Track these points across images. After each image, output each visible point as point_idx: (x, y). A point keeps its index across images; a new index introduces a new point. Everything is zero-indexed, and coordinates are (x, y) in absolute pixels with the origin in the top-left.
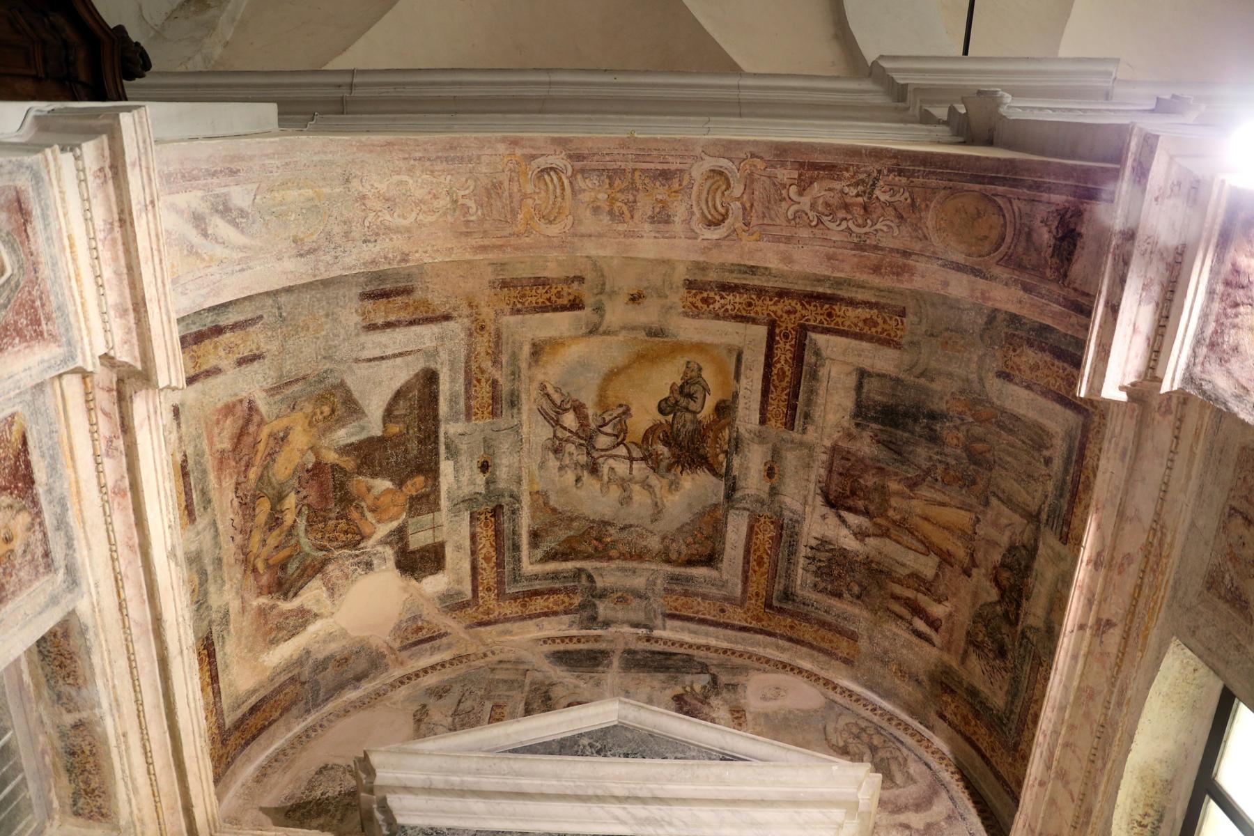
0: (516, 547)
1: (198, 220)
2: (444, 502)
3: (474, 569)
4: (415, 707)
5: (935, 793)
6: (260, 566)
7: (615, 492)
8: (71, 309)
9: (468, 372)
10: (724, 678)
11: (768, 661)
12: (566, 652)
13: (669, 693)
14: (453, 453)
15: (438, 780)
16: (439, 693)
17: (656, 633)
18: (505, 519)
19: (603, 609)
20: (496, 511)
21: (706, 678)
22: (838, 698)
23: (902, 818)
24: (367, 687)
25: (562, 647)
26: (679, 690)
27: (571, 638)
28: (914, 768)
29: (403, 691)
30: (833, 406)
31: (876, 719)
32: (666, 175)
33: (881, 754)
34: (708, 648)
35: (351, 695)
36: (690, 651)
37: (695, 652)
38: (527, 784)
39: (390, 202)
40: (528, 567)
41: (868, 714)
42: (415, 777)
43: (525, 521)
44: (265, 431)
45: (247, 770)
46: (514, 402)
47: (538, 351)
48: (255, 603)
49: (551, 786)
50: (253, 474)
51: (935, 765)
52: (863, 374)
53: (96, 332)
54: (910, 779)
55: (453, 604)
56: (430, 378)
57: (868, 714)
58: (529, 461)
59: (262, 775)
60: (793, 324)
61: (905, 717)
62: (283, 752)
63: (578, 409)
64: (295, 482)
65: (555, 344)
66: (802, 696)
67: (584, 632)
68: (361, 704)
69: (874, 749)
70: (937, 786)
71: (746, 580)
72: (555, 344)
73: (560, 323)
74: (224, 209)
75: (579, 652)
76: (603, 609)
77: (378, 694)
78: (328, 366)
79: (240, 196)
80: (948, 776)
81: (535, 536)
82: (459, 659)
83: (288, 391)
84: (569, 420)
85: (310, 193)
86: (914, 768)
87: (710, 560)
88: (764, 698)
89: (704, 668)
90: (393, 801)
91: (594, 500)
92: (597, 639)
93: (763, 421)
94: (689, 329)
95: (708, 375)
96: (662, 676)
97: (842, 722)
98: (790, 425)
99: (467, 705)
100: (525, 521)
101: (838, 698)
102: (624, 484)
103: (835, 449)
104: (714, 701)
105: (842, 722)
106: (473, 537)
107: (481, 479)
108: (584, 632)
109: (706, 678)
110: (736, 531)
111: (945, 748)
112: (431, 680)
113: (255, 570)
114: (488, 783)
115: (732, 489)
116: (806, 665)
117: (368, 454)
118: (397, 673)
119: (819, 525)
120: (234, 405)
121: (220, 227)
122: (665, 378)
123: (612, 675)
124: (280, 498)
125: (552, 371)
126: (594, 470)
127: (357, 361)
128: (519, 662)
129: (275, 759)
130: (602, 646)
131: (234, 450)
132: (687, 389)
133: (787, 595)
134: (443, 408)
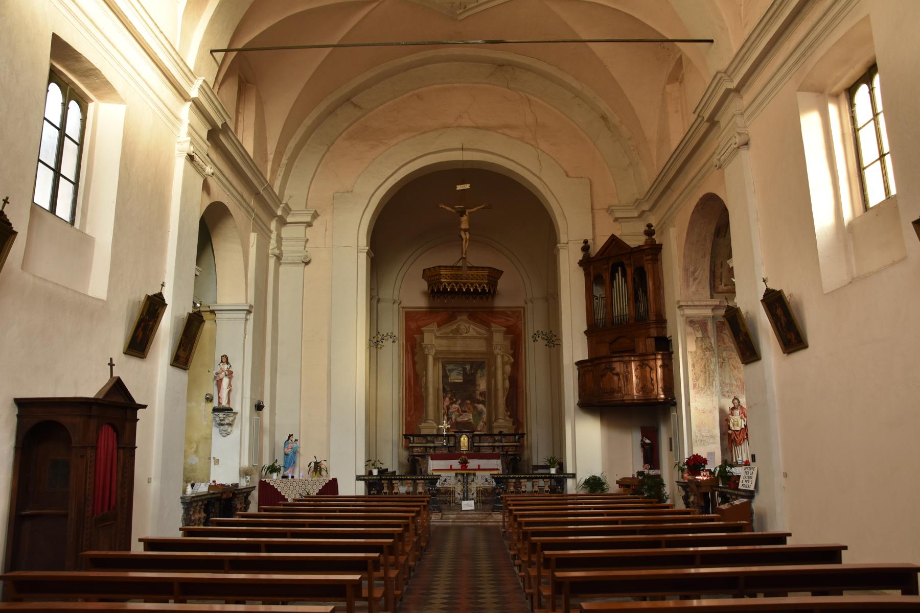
1: (695, 280)
53: (708, 312)
74: (694, 272)
79: (692, 269)
121: (697, 274)
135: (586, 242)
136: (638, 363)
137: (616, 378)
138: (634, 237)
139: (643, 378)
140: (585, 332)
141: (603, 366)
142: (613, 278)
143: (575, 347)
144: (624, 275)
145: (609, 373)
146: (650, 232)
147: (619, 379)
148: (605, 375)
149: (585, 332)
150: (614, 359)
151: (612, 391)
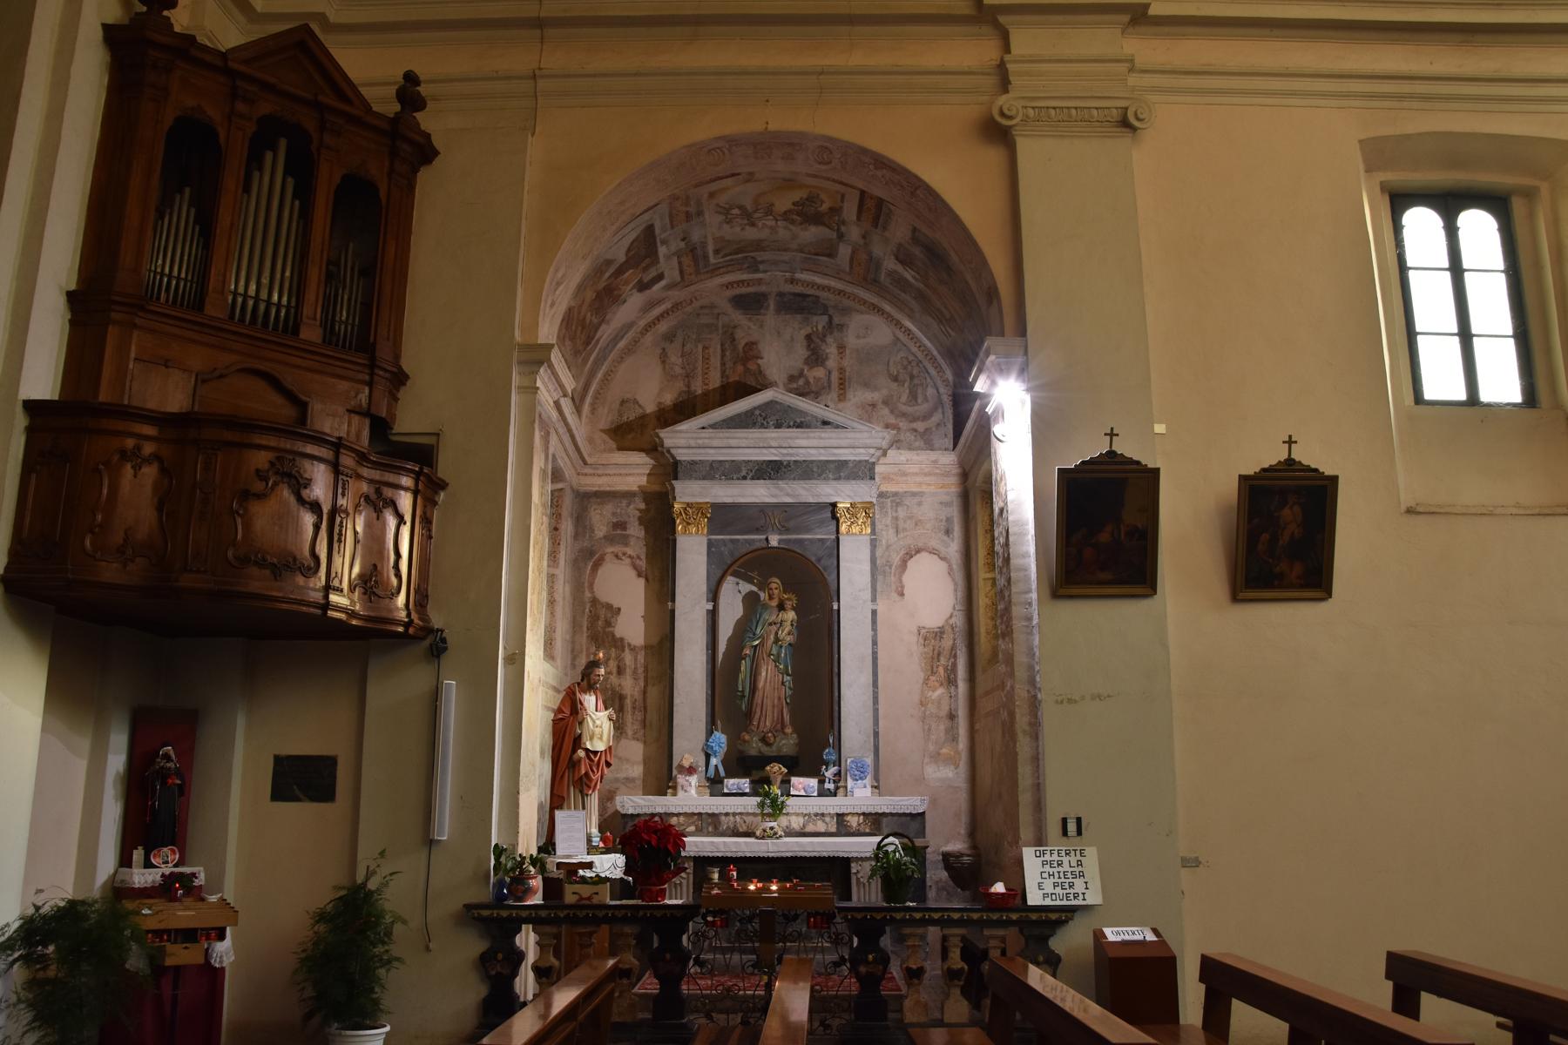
0: (706, 257)
2: (662, 259)
3: (681, 272)
4: (659, 351)
5: (935, 409)
7: (767, 231)
9: (671, 216)
10: (836, 320)
11: (865, 302)
12: (741, 296)
13: (804, 332)
14: (664, 242)
15: (692, 443)
16: (669, 337)
17: (798, 276)
18: (699, 252)
19: (761, 267)
20: (693, 250)
21: (826, 318)
22: (901, 336)
23: (914, 425)
24: (630, 335)
25: (738, 291)
26: (809, 330)
27: (743, 282)
28: (930, 391)
29: (649, 338)
30: (899, 231)
31: (919, 354)
32: (790, 144)
33: (916, 381)
34: (829, 289)
35: (622, 344)
36: (817, 293)
37: (823, 295)
38: (733, 442)
40: (712, 260)
41: (914, 350)
42: (682, 442)
43: (710, 248)
45: (586, 408)
46: (700, 213)
47: (712, 195)
49: (744, 443)
51: (942, 390)
52: (915, 230)
54: (926, 399)
55: (669, 287)
56: (650, 229)
57: (914, 350)
58: (711, 229)
59: (593, 410)
60: (875, 212)
61: (935, 353)
62: (597, 393)
63: (740, 207)
65: (723, 190)
66: (881, 334)
67: (751, 276)
68: (629, 351)
69: (912, 377)
70: (940, 403)
71: (851, 267)
72: (723, 190)
73: (729, 182)
74: (558, 284)
75: (748, 295)
76: (761, 267)
77: (636, 341)
79: (560, 275)
80: (947, 399)
81: (717, 252)
82: (676, 306)
84: (736, 211)
86: (930, 391)
87: (830, 255)
88: (858, 337)
89: (825, 310)
90: (673, 451)
91: (751, 234)
92: (760, 282)
93: (859, 219)
94: (810, 181)
95: (823, 196)
96: (799, 317)
97: (902, 354)
98: (875, 223)
99: (688, 347)
100: (710, 248)
101: (901, 336)
102: (771, 227)
103: (900, 245)
104: (829, 340)
105: (902, 354)
106: (680, 263)
107: (682, 245)
108: (751, 276)
109: (826, 318)
110: (844, 251)
111: (951, 378)
112: (663, 327)
114: (716, 443)
115: (841, 236)
116: (887, 308)
117: (620, 271)
118: (642, 323)
119: (890, 264)
122: (797, 195)
123: (770, 318)
125: (723, 199)
126: (753, 225)
128: (713, 306)
129: (595, 398)
130: (763, 289)
132: (812, 199)
133: (875, 281)
134: (657, 231)
136: (365, 487)
137: (308, 519)
139: (374, 544)
141: (261, 459)
145: (286, 493)
146: (410, 93)
148: (261, 496)
150: (310, 449)
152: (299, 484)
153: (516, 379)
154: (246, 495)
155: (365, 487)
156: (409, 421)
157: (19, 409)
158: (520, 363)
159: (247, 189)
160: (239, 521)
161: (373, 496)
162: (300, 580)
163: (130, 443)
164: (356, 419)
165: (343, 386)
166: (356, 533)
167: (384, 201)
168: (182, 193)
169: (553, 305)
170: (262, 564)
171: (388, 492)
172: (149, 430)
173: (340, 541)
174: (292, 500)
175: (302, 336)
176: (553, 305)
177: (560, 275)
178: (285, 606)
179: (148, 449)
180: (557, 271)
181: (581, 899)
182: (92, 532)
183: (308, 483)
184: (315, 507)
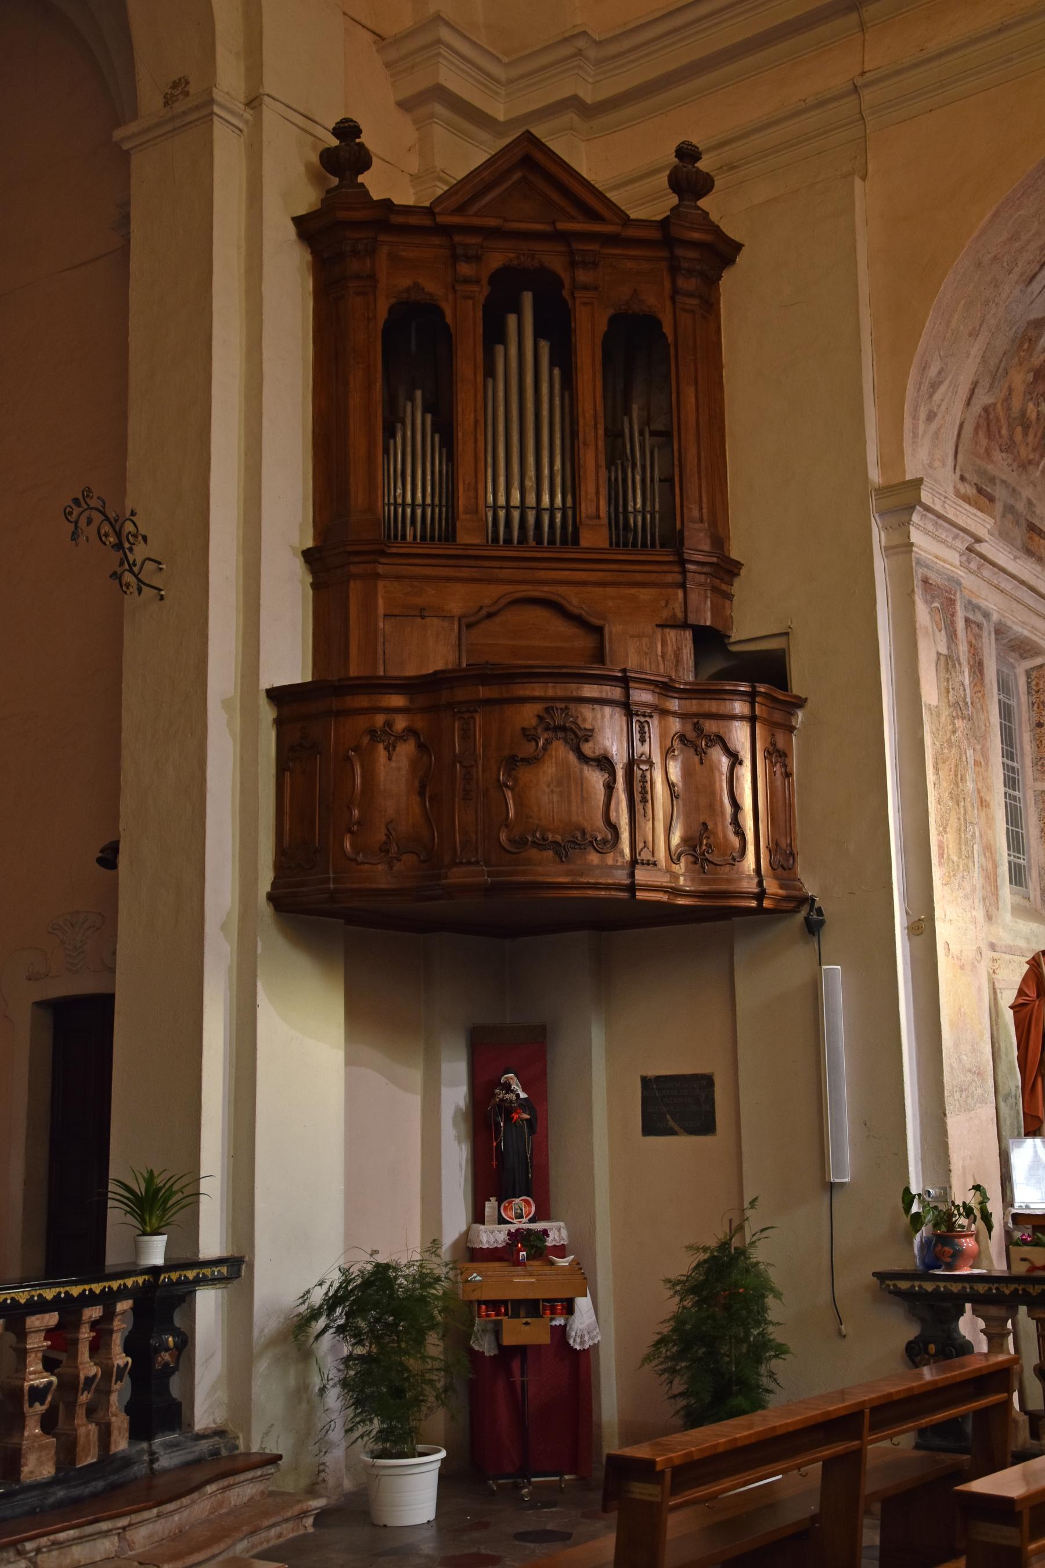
6: (1031, 457)
8: (949, 572)
39: (1014, 237)
44: (999, 405)
48: (1038, 473)
50: (1004, 431)
64: (1028, 397)
74: (934, 386)
78: (1014, 329)
83: (1000, 371)
85: (963, 302)
113: (1030, 462)
120: (978, 423)
124: (1023, 413)
127: (1031, 303)
131: (989, 439)
135: (347, 130)
136: (675, 725)
137: (596, 779)
138: (621, 166)
139: (699, 799)
140: (308, 555)
141: (528, 714)
142: (494, 334)
143: (256, 624)
144: (556, 327)
145: (561, 751)
146: (688, 178)
147: (610, 788)
148: (532, 761)
149: (308, 555)
150: (589, 691)
151: (575, 841)
152: (577, 737)
153: (878, 537)
154: (513, 763)
155: (675, 725)
156: (749, 627)
157: (263, 700)
158: (882, 514)
159: (490, 371)
160: (509, 794)
161: (691, 734)
162: (594, 858)
163: (380, 719)
164: (672, 634)
165: (645, 595)
166: (671, 785)
167: (671, 339)
168: (412, 399)
169: (931, 417)
170: (542, 845)
171: (711, 727)
172: (398, 701)
173: (644, 801)
174: (572, 757)
175: (584, 543)
176: (931, 417)
177: (933, 371)
178: (576, 893)
179: (401, 723)
180: (924, 368)
181: (1033, 1268)
182: (352, 833)
183: (588, 735)
184: (605, 763)
